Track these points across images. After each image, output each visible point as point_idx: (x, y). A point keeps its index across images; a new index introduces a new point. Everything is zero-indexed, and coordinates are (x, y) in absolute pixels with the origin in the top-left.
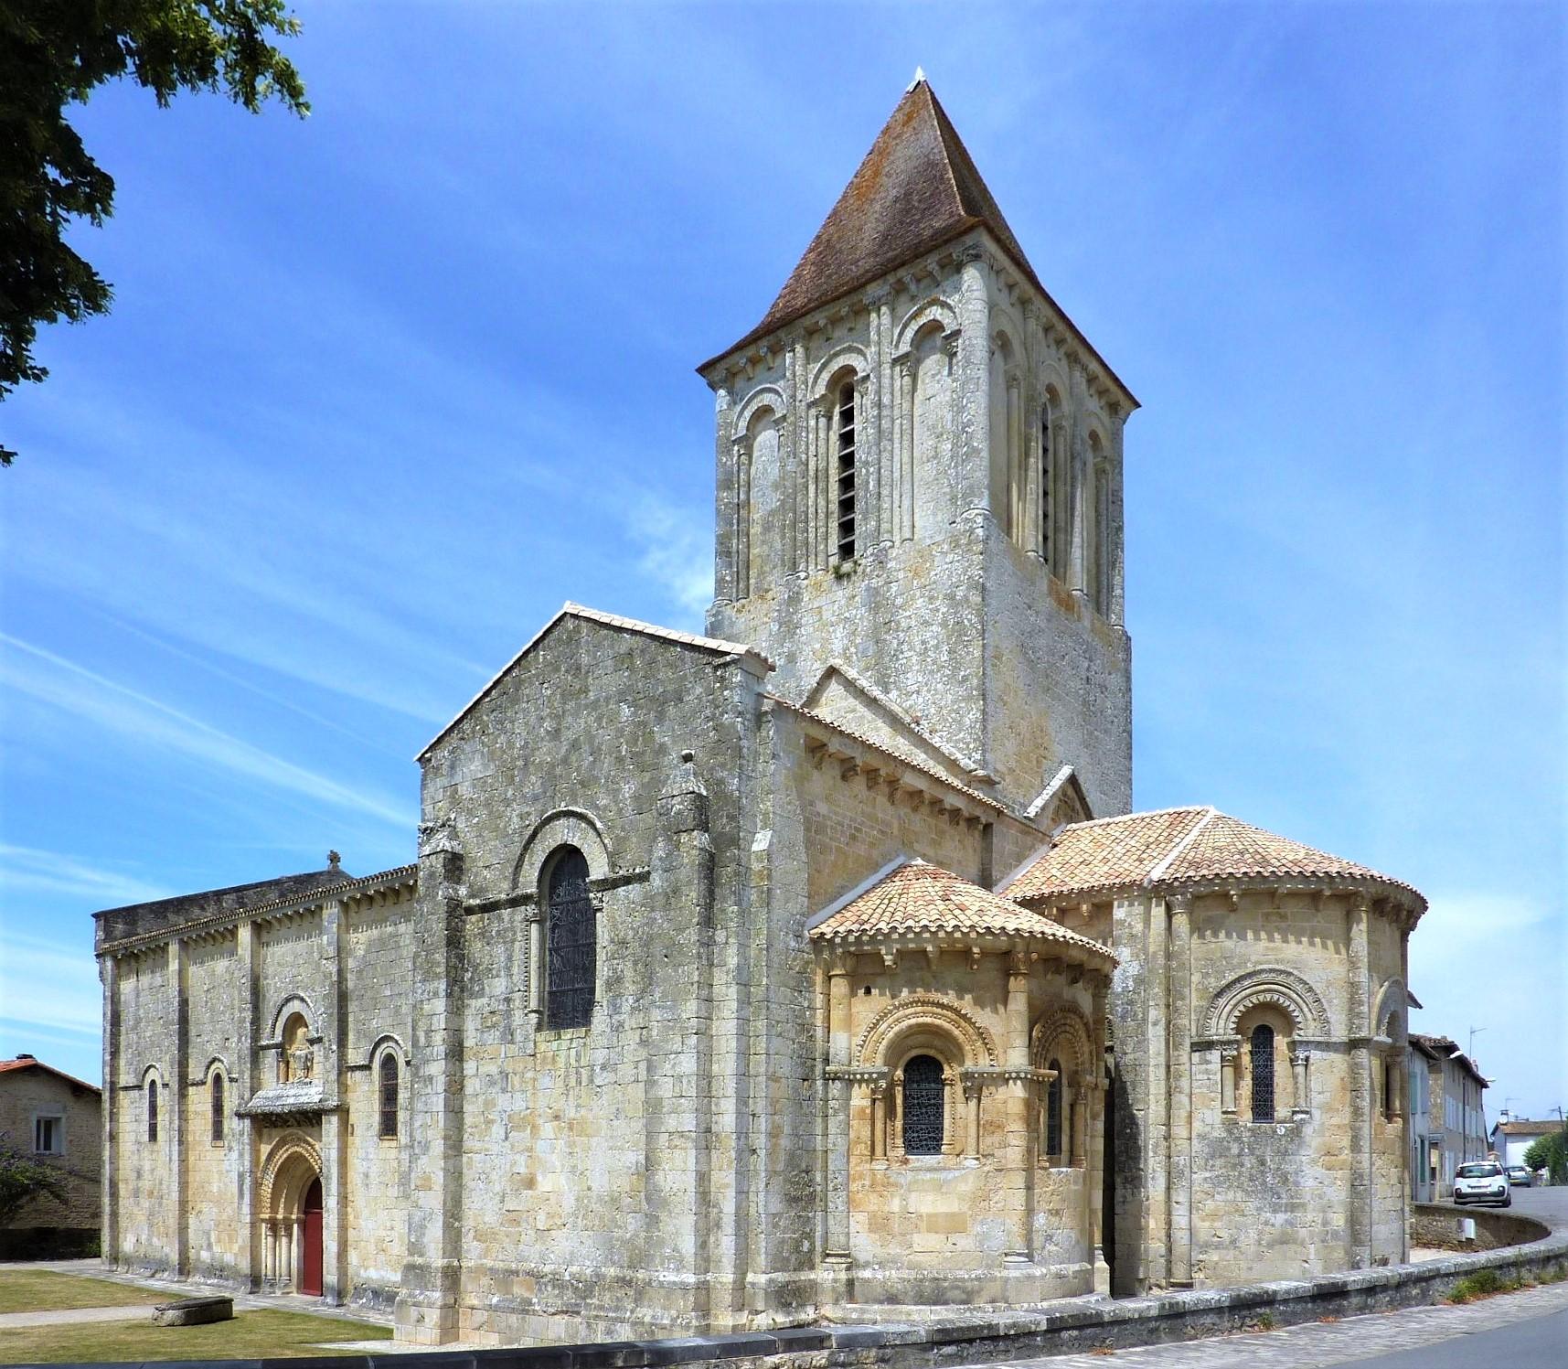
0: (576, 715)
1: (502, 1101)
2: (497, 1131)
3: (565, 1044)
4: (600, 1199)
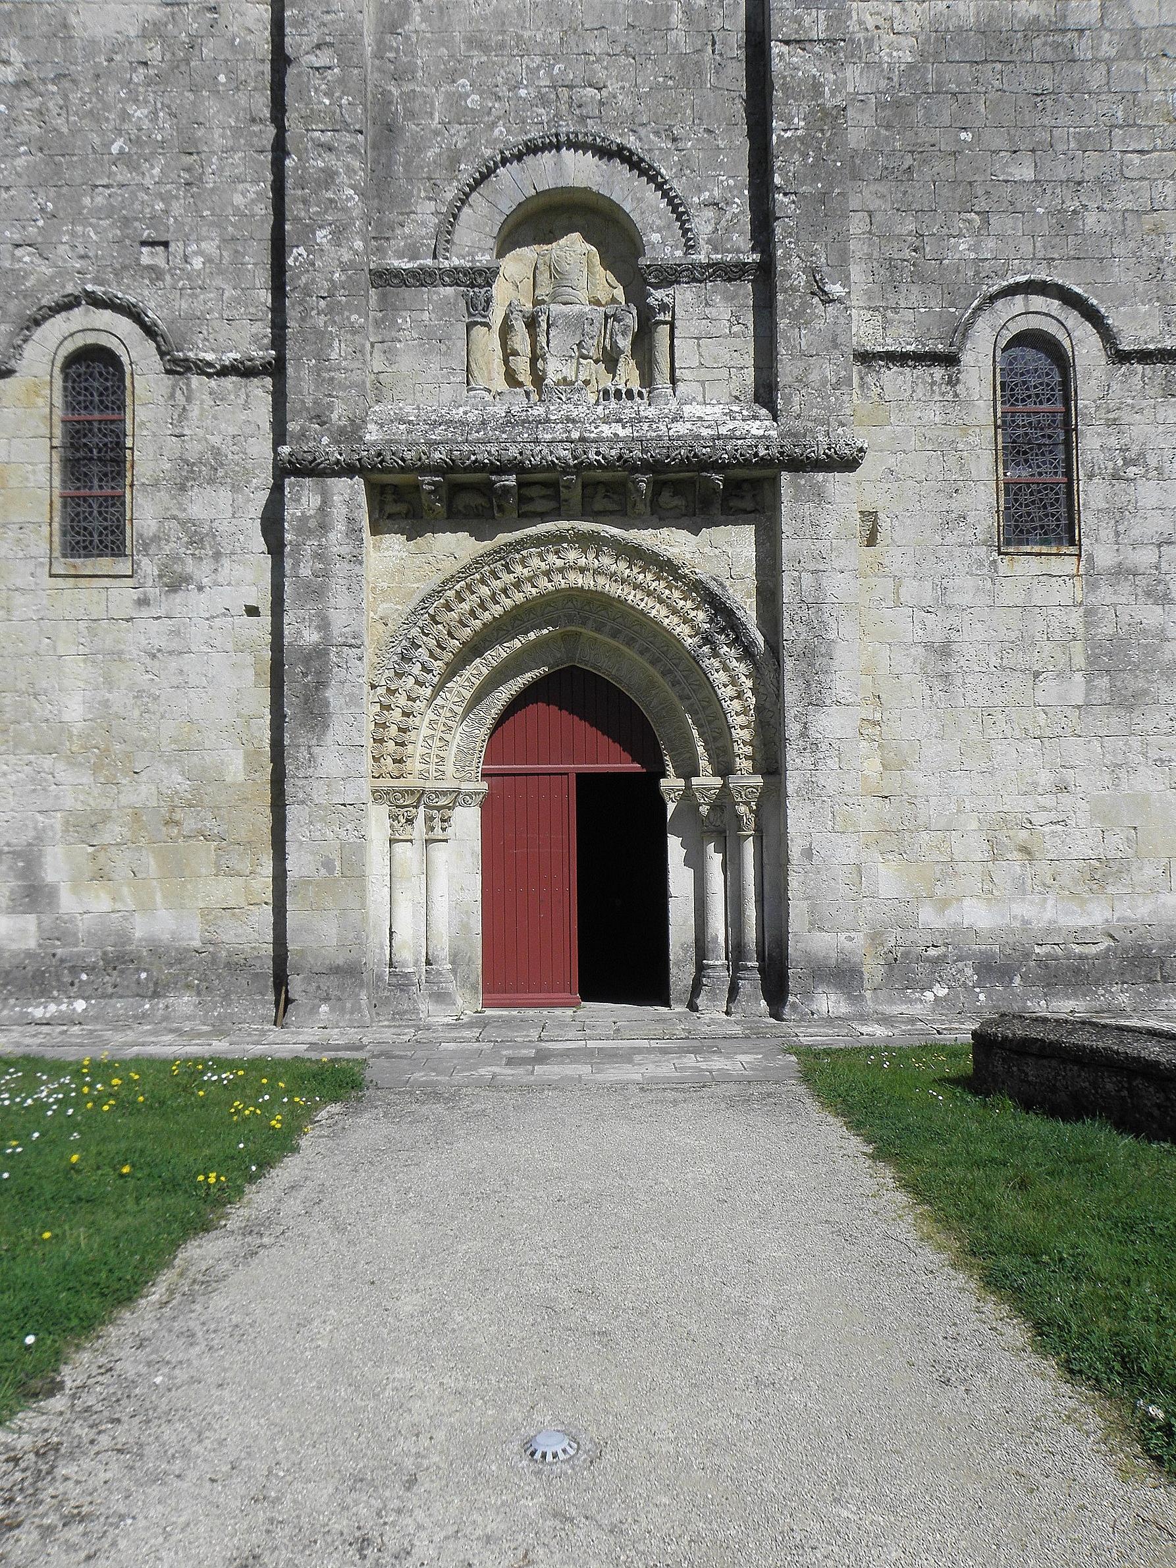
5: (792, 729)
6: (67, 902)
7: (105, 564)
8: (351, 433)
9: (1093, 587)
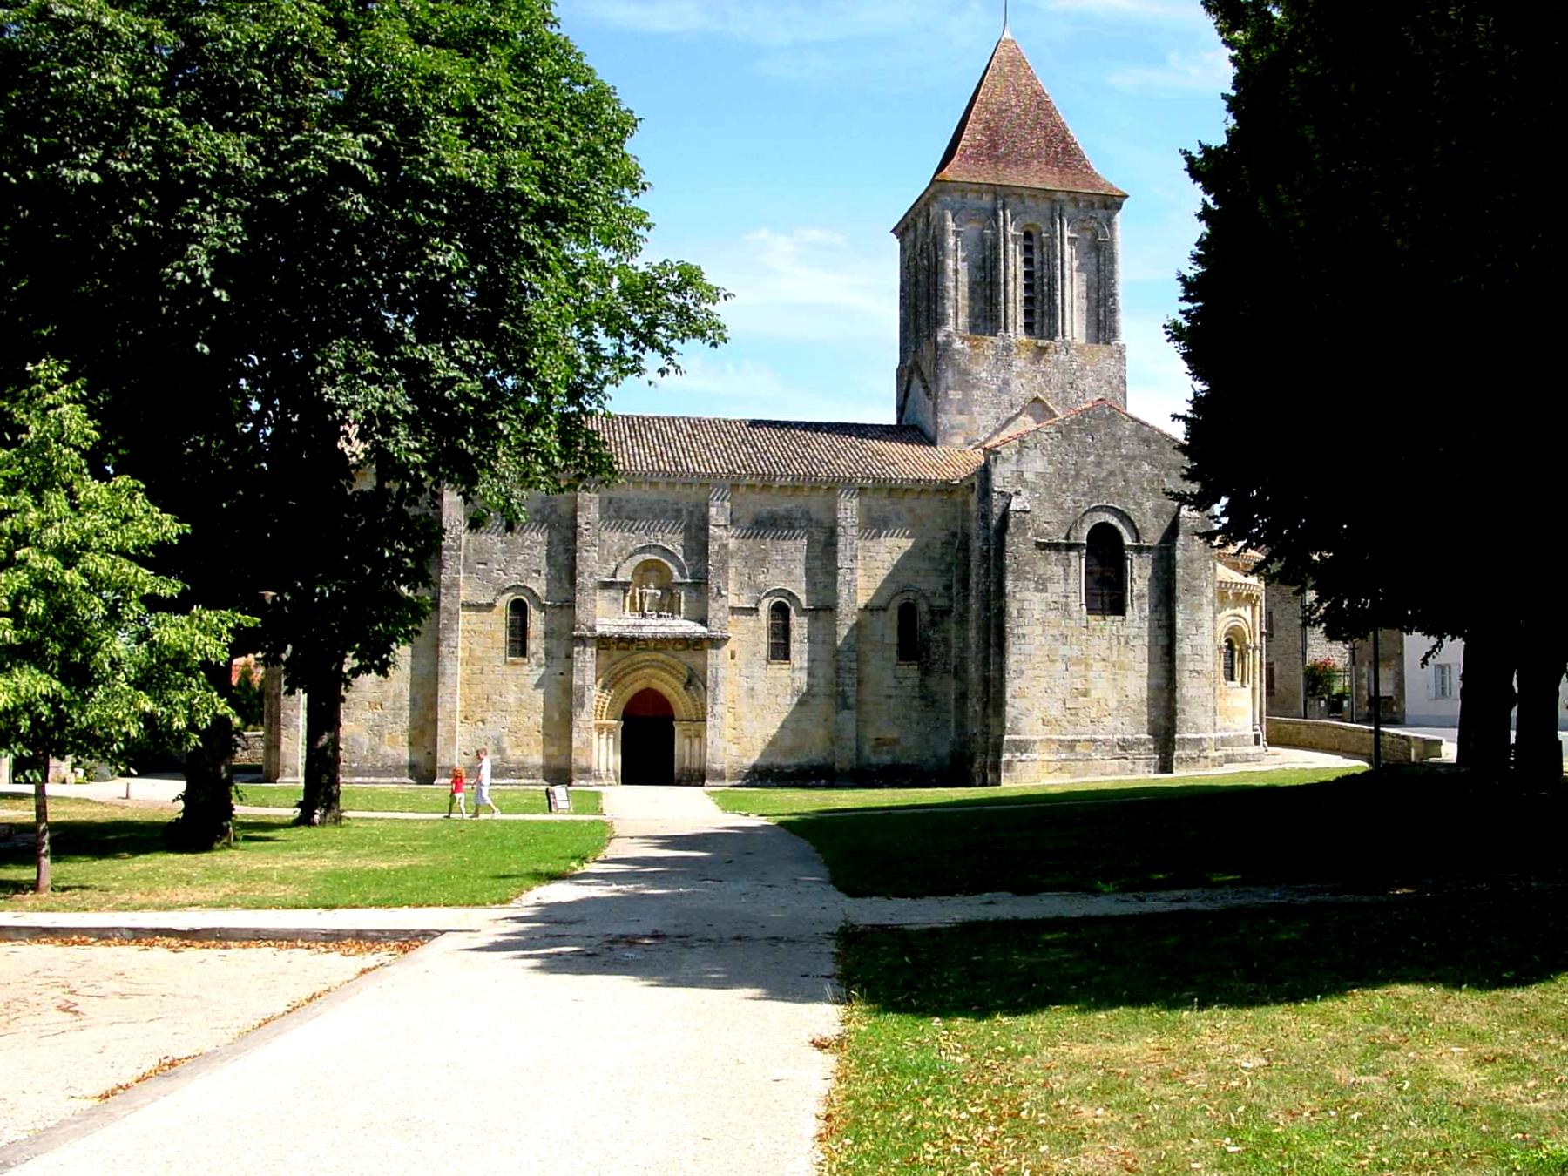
0: (1113, 457)
1: (1064, 650)
2: (1060, 666)
3: (1109, 623)
4: (1133, 702)
5: (709, 710)
6: (509, 752)
7: (520, 660)
8: (592, 629)
9: (793, 671)
